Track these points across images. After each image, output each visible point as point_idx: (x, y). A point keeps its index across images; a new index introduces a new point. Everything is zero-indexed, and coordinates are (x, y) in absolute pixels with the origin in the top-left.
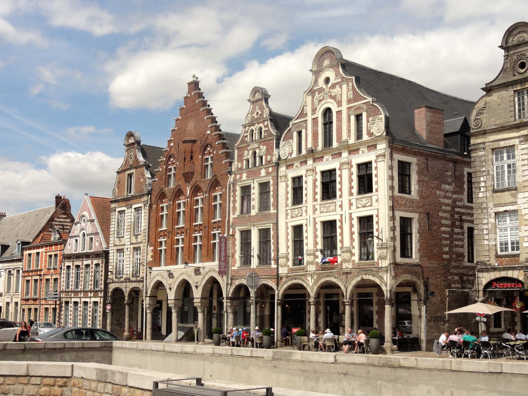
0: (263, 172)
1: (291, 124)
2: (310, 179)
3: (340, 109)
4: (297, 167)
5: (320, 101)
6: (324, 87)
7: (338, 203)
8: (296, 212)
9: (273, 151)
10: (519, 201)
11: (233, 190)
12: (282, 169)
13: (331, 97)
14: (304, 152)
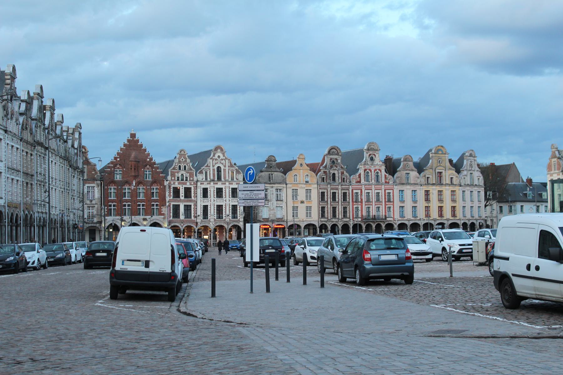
0: (188, 183)
1: (202, 168)
2: (212, 190)
3: (225, 168)
4: (206, 184)
5: (216, 164)
6: (218, 159)
7: (224, 200)
8: (206, 200)
9: (193, 176)
10: (269, 204)
11: (169, 188)
12: (199, 184)
13: (221, 163)
14: (209, 179)
